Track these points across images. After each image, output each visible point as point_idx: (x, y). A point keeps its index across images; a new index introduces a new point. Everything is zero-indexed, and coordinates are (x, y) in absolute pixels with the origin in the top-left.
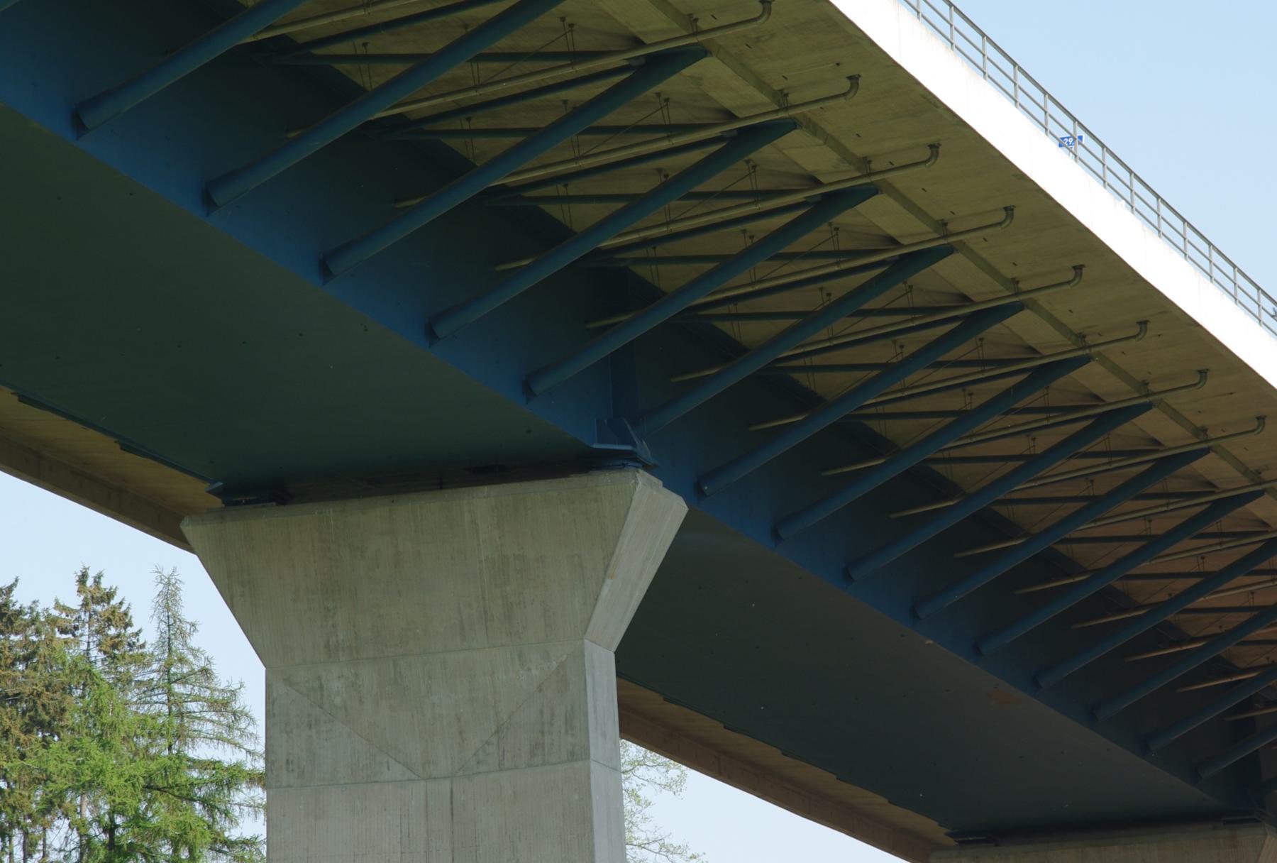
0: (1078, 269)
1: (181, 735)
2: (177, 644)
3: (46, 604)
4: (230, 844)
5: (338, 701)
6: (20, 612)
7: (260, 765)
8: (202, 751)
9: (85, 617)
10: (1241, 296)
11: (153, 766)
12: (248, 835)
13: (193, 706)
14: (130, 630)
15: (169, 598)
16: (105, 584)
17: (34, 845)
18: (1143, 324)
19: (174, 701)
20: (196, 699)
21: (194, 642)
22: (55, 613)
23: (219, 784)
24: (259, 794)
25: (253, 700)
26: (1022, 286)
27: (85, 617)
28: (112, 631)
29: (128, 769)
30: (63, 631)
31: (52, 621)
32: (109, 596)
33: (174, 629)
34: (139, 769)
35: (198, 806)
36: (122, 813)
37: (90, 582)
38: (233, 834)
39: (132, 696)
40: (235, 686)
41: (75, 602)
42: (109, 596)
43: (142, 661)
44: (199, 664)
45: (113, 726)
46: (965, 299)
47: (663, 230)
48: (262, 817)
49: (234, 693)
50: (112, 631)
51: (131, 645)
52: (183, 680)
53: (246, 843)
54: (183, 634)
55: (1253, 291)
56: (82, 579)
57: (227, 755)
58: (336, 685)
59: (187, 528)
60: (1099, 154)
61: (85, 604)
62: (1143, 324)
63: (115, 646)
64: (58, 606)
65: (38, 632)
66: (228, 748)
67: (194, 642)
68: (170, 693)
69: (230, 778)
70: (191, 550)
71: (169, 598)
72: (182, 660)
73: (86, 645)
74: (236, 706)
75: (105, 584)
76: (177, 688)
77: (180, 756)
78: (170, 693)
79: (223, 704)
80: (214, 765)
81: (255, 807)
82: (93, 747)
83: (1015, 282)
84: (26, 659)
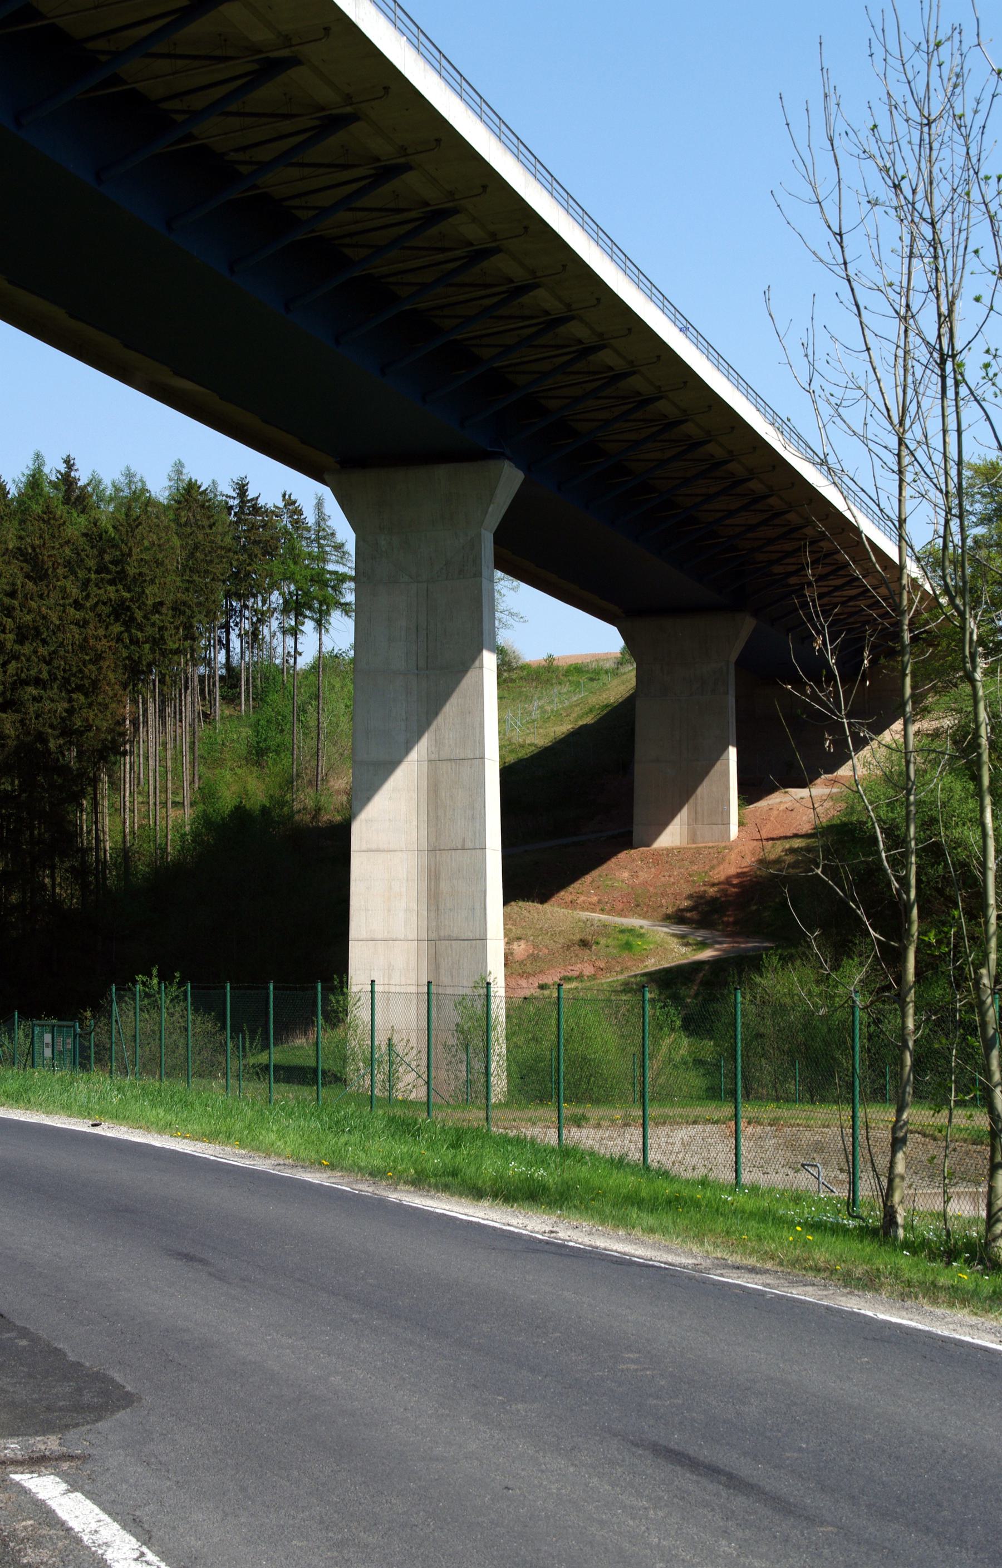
0: (685, 383)
1: (325, 561)
2: (322, 523)
3: (270, 505)
4: (342, 604)
5: (384, 549)
6: (261, 508)
7: (353, 573)
8: (331, 567)
9: (285, 511)
10: (749, 397)
11: (313, 572)
12: (348, 601)
13: (328, 549)
14: (302, 517)
15: (319, 505)
16: (293, 498)
17: (266, 603)
18: (710, 407)
19: (320, 546)
20: (329, 546)
21: (328, 523)
22: (273, 508)
23: (338, 580)
24: (352, 585)
25: (351, 547)
26: (662, 389)
27: (285, 511)
28: (296, 517)
29: (304, 573)
30: (276, 516)
31: (273, 512)
32: (295, 502)
33: (321, 517)
34: (308, 573)
35: (330, 589)
36: (301, 590)
37: (287, 497)
38: (343, 601)
39: (304, 543)
40: (344, 542)
41: (281, 505)
42: (295, 502)
43: (308, 529)
44: (329, 532)
45: (299, 555)
46: (639, 394)
47: (519, 360)
48: (354, 593)
49: (343, 545)
50: (296, 517)
51: (303, 523)
52: (324, 538)
53: (346, 604)
54: (324, 519)
55: (754, 395)
56: (284, 495)
57: (341, 569)
58: (383, 543)
59: (326, 477)
60: (662, 300)
61: (285, 506)
62: (710, 407)
63: (297, 523)
64: (275, 506)
65: (267, 516)
66: (341, 566)
67: (328, 523)
68: (319, 543)
69: (343, 578)
70: (327, 485)
71: (319, 505)
72: (324, 530)
73: (285, 520)
74: (345, 549)
75: (293, 498)
76: (322, 541)
77: (323, 569)
78: (319, 543)
79: (339, 547)
80: (336, 573)
81: (351, 590)
82: (290, 562)
83: (660, 387)
84: (263, 527)
